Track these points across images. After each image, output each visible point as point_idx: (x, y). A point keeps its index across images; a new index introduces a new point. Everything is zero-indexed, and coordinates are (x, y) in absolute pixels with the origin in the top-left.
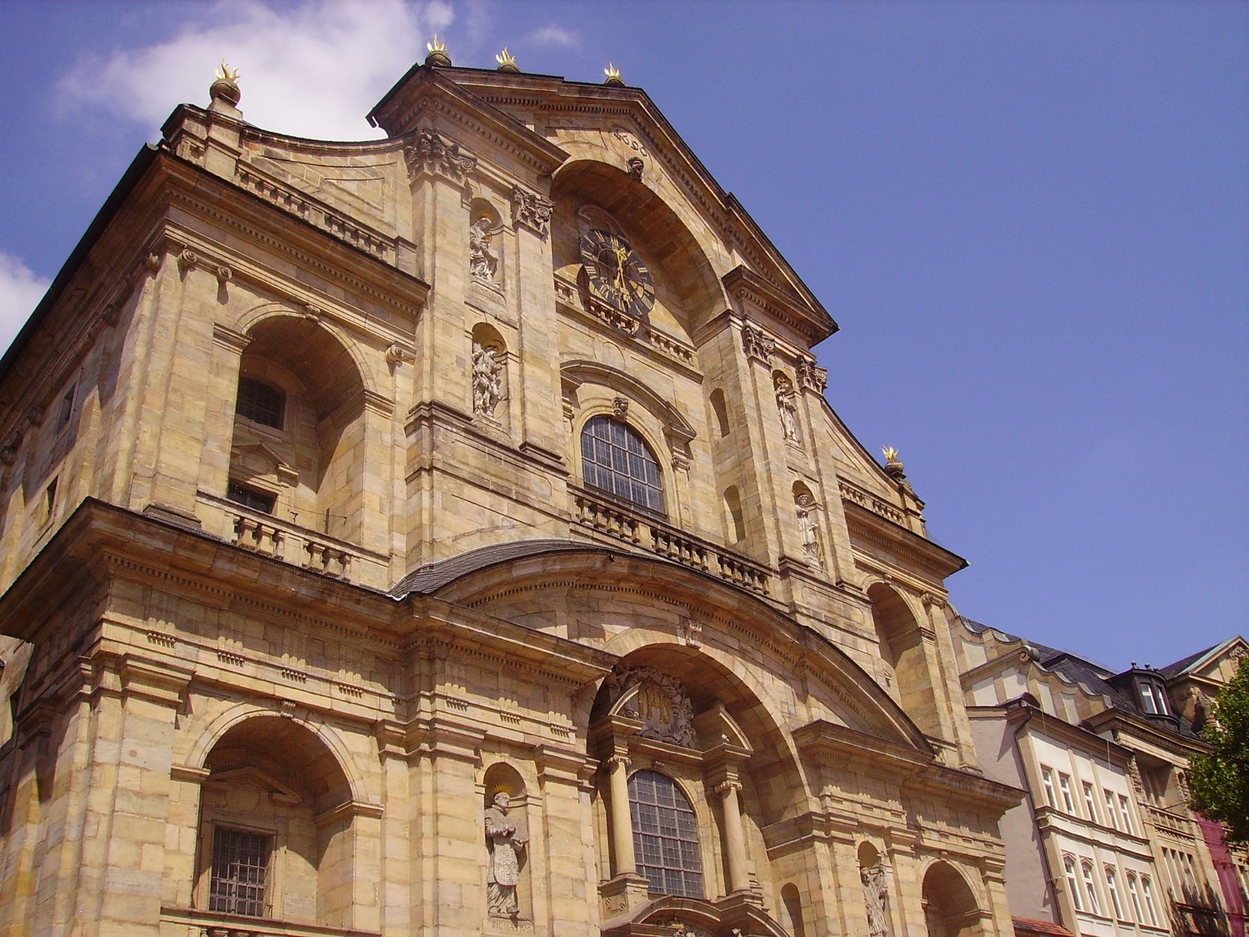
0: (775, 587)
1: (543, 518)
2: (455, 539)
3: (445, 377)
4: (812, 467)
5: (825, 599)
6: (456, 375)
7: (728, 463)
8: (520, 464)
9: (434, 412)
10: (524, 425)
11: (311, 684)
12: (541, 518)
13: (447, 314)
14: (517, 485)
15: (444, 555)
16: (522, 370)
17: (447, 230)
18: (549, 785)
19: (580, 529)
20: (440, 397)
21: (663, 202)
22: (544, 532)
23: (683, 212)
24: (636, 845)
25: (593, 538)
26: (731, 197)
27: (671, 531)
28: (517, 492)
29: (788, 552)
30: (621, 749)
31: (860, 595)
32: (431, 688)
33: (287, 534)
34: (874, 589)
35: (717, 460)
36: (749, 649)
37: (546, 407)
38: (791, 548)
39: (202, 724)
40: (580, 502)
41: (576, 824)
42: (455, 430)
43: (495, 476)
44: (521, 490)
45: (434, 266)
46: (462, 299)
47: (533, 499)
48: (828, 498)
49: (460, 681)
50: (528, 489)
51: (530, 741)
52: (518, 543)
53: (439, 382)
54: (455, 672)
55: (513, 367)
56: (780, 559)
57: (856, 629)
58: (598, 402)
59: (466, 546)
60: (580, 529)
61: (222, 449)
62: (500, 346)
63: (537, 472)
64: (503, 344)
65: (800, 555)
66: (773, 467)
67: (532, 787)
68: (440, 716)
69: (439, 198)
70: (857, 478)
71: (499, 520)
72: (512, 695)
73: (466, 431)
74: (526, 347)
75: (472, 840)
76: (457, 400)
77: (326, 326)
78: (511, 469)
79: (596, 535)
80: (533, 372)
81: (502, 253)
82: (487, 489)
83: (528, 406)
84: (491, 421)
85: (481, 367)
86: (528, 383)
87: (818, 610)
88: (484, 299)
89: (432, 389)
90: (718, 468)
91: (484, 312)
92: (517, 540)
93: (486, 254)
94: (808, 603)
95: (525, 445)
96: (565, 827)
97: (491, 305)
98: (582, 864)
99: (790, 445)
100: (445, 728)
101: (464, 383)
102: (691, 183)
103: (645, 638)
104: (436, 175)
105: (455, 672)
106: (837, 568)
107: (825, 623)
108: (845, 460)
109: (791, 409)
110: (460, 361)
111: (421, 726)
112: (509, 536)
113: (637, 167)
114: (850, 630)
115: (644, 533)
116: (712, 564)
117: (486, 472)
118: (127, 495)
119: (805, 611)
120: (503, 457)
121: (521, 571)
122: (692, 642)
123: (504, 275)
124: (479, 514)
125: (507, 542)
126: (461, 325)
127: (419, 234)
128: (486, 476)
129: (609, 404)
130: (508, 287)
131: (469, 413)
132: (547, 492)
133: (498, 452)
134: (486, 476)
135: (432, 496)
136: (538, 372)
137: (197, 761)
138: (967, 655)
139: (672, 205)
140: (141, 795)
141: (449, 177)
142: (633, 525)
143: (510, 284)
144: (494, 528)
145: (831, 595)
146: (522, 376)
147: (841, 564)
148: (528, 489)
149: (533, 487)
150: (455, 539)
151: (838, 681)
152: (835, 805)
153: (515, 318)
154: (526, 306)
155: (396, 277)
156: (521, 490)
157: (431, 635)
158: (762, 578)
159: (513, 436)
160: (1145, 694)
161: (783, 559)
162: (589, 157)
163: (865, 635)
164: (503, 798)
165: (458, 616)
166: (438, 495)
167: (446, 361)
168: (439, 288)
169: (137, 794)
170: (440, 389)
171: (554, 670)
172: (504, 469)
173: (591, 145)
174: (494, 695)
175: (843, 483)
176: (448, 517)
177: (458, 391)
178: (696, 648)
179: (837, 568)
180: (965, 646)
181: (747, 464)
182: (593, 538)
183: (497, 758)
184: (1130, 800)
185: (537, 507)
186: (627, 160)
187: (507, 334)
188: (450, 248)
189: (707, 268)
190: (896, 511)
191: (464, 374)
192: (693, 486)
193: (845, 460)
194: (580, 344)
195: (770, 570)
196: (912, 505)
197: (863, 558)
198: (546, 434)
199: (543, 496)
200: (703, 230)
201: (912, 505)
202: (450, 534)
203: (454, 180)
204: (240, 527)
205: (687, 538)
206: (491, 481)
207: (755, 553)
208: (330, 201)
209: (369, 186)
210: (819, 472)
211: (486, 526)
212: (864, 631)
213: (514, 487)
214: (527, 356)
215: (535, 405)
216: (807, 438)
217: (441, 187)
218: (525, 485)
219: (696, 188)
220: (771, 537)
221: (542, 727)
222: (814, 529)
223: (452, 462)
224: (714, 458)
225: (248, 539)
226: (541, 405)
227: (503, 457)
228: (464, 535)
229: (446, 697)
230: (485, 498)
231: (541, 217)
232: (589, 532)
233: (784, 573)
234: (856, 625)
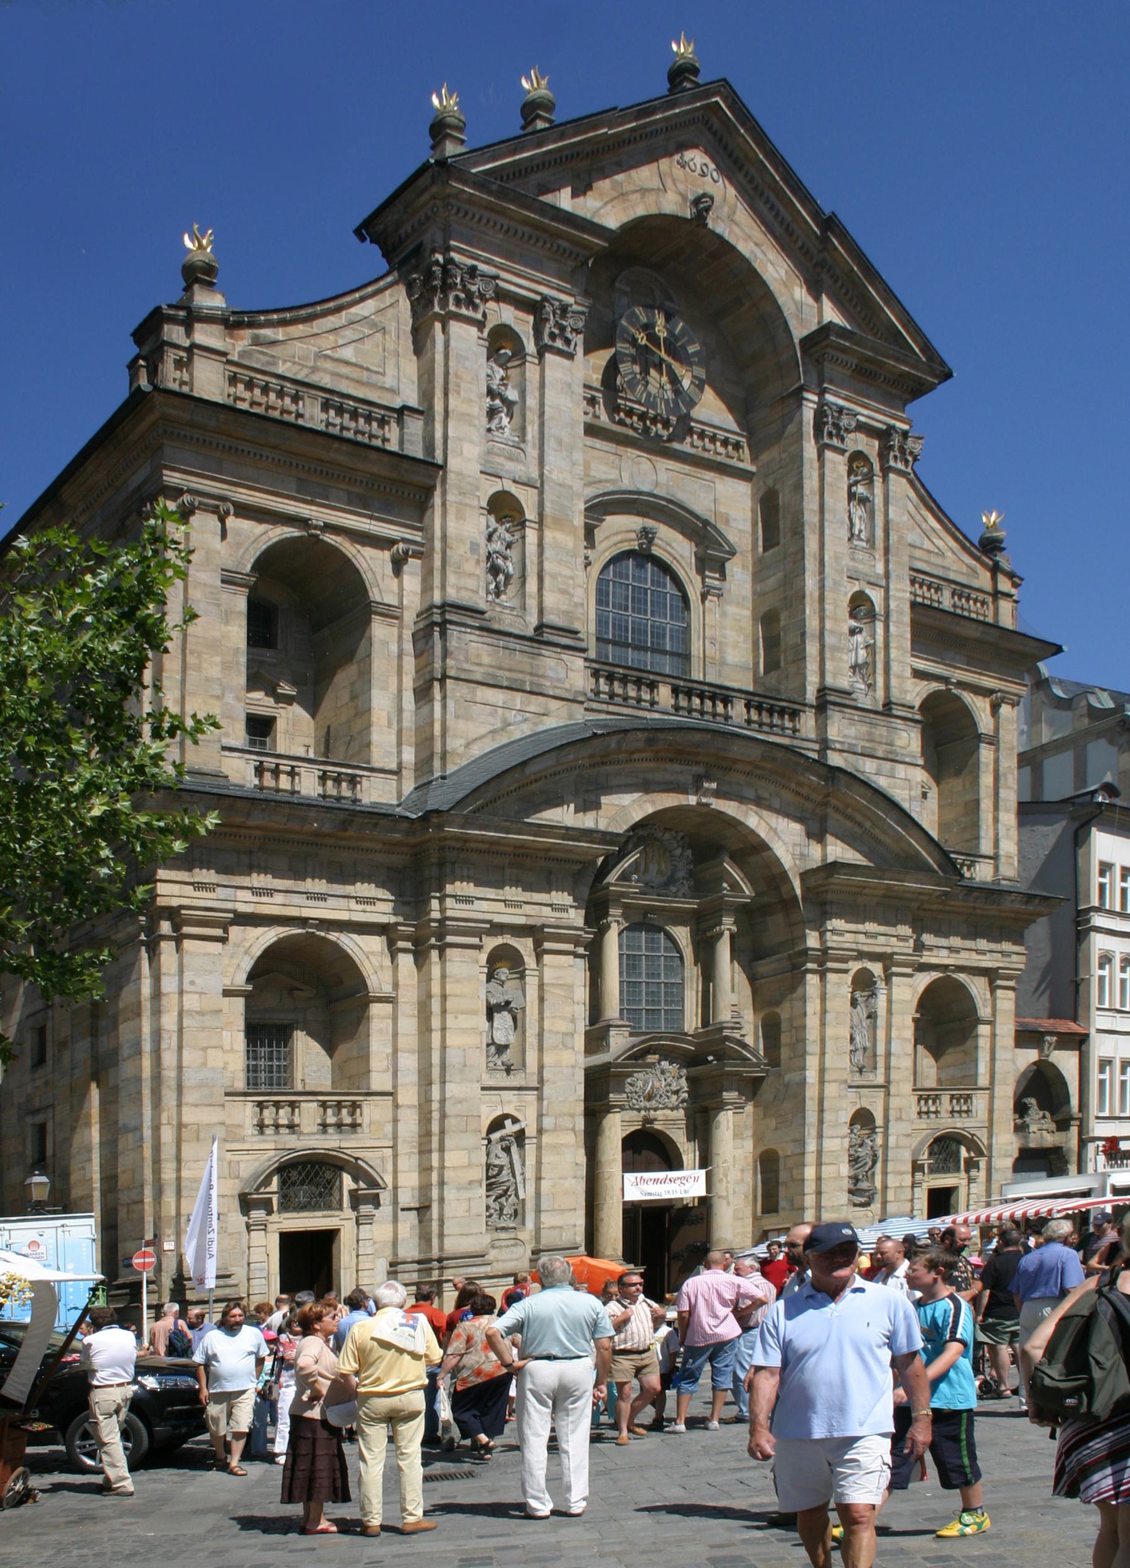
1: (559, 703)
2: (467, 745)
3: (459, 573)
4: (880, 568)
5: (864, 728)
6: (469, 567)
7: (772, 582)
8: (536, 651)
9: (448, 617)
12: (554, 705)
13: (460, 494)
14: (531, 674)
15: (455, 764)
17: (462, 385)
18: (547, 958)
19: (595, 705)
20: (453, 595)
21: (732, 249)
23: (760, 255)
25: (608, 713)
27: (695, 685)
28: (531, 683)
29: (829, 681)
31: (910, 716)
32: (441, 888)
34: (930, 704)
36: (767, 795)
37: (566, 577)
38: (835, 676)
40: (596, 674)
42: (469, 630)
43: (510, 670)
44: (535, 679)
46: (479, 468)
47: (548, 686)
49: (468, 879)
50: (543, 676)
51: (531, 922)
52: (530, 736)
53: (451, 578)
54: (465, 873)
55: (531, 535)
56: (819, 691)
57: (897, 754)
59: (477, 751)
60: (595, 705)
62: (517, 515)
63: (553, 655)
64: (521, 511)
65: (844, 683)
67: (530, 961)
68: (449, 913)
69: (452, 343)
70: (937, 565)
71: (511, 716)
72: (516, 882)
73: (481, 629)
74: (548, 510)
75: (475, 1013)
76: (470, 594)
78: (525, 659)
79: (611, 708)
80: (554, 538)
81: (523, 393)
82: (501, 687)
83: (547, 581)
84: (505, 607)
85: (497, 546)
86: (548, 553)
87: (854, 742)
88: (501, 460)
89: (443, 587)
91: (500, 478)
92: (529, 733)
93: (504, 400)
94: (845, 736)
95: (540, 628)
96: (559, 992)
97: (510, 466)
100: (454, 923)
101: (478, 572)
103: (653, 802)
104: (450, 312)
105: (465, 873)
106: (887, 687)
107: (862, 755)
108: (927, 545)
109: (863, 501)
110: (474, 547)
111: (433, 924)
113: (702, 205)
114: (891, 756)
115: (664, 694)
117: (500, 668)
119: (838, 746)
120: (518, 647)
121: (530, 770)
122: (704, 800)
123: (524, 421)
124: (491, 715)
125: (518, 737)
126: (476, 503)
128: (500, 673)
130: (529, 437)
131: (482, 606)
132: (562, 675)
133: (513, 643)
134: (500, 673)
135: (444, 707)
136: (559, 536)
137: (240, 980)
139: (744, 248)
141: (464, 311)
142: (652, 686)
143: (532, 431)
144: (506, 724)
145: (874, 721)
146: (541, 545)
148: (543, 676)
149: (550, 673)
150: (467, 745)
151: (864, 816)
154: (550, 457)
155: (405, 465)
156: (535, 679)
157: (443, 844)
158: (794, 715)
159: (528, 618)
161: (823, 690)
162: (640, 211)
163: (907, 760)
164: (503, 972)
166: (450, 704)
167: (460, 551)
168: (453, 464)
170: (452, 586)
171: (559, 855)
172: (519, 659)
173: (644, 191)
174: (499, 885)
175: (918, 577)
176: (461, 725)
177: (471, 583)
178: (707, 805)
179: (887, 687)
182: (608, 713)
183: (499, 941)
185: (551, 693)
186: (691, 197)
187: (527, 499)
188: (465, 408)
190: (981, 596)
191: (478, 562)
195: (805, 705)
196: (1004, 585)
197: (922, 665)
198: (564, 608)
199: (559, 680)
200: (783, 273)
201: (1004, 585)
202: (463, 742)
203: (469, 313)
205: (711, 689)
206: (504, 677)
207: (787, 689)
212: (907, 756)
213: (528, 678)
214: (548, 521)
215: (554, 577)
217: (455, 327)
218: (540, 672)
220: (812, 667)
221: (543, 908)
222: (867, 647)
226: (561, 575)
227: (518, 647)
228: (476, 739)
229: (454, 896)
231: (573, 330)
232: (604, 707)
234: (898, 750)
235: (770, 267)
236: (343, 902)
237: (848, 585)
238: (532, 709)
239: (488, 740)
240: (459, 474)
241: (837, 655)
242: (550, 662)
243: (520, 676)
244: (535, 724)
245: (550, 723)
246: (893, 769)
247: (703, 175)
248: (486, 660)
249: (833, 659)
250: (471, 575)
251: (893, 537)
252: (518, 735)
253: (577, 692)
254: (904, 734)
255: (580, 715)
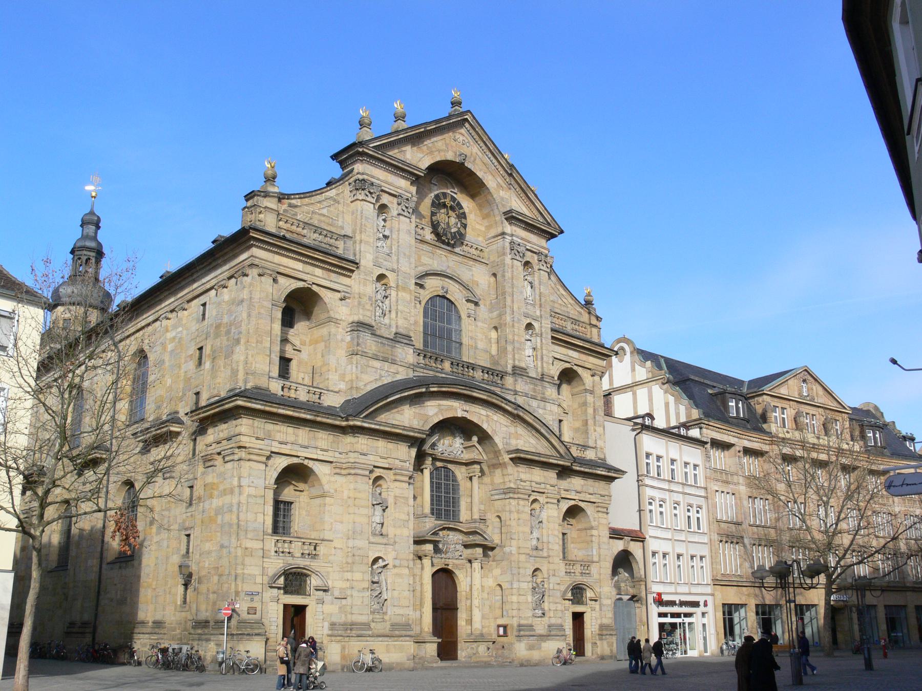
0: (509, 381)
4: (538, 313)
5: (532, 386)
10: (397, 323)
11: (310, 450)
12: (401, 369)
16: (397, 295)
21: (475, 174)
22: (403, 374)
24: (432, 500)
26: (512, 166)
29: (517, 363)
30: (429, 461)
33: (300, 388)
35: (491, 311)
39: (273, 469)
41: (407, 499)
45: (360, 249)
46: (372, 264)
48: (543, 330)
58: (433, 289)
61: (276, 356)
65: (523, 365)
66: (516, 319)
71: (383, 373)
73: (372, 334)
77: (315, 288)
83: (399, 313)
88: (382, 261)
90: (490, 315)
97: (385, 263)
98: (408, 515)
99: (527, 303)
102: (492, 158)
106: (542, 367)
112: (387, 380)
115: (447, 365)
116: (478, 375)
118: (246, 382)
127: (354, 232)
129: (438, 289)
136: (404, 294)
138: (637, 372)
139: (480, 174)
140: (255, 497)
144: (381, 376)
147: (545, 365)
150: (365, 385)
152: (522, 483)
153: (395, 267)
160: (730, 404)
161: (514, 367)
162: (438, 159)
165: (365, 422)
169: (254, 496)
179: (542, 367)
180: (637, 367)
181: (503, 317)
184: (701, 466)
189: (496, 207)
191: (372, 304)
192: (477, 326)
193: (560, 301)
194: (427, 259)
202: (363, 383)
204: (283, 388)
208: (316, 223)
209: (332, 209)
210: (541, 317)
211: (378, 377)
216: (537, 297)
219: (494, 161)
223: (365, 350)
224: (489, 309)
225: (286, 393)
230: (377, 364)
233: (514, 374)
235: (490, 183)
236: (314, 450)
237: (524, 320)
238: (392, 370)
239: (374, 383)
240: (365, 267)
241: (520, 352)
242: (400, 351)
243: (387, 356)
244: (393, 377)
245: (399, 377)
246: (545, 406)
247: (463, 144)
248: (374, 348)
249: (518, 353)
250: (369, 310)
251: (543, 300)
252: (386, 382)
253: (410, 364)
254: (549, 390)
255: (411, 374)
